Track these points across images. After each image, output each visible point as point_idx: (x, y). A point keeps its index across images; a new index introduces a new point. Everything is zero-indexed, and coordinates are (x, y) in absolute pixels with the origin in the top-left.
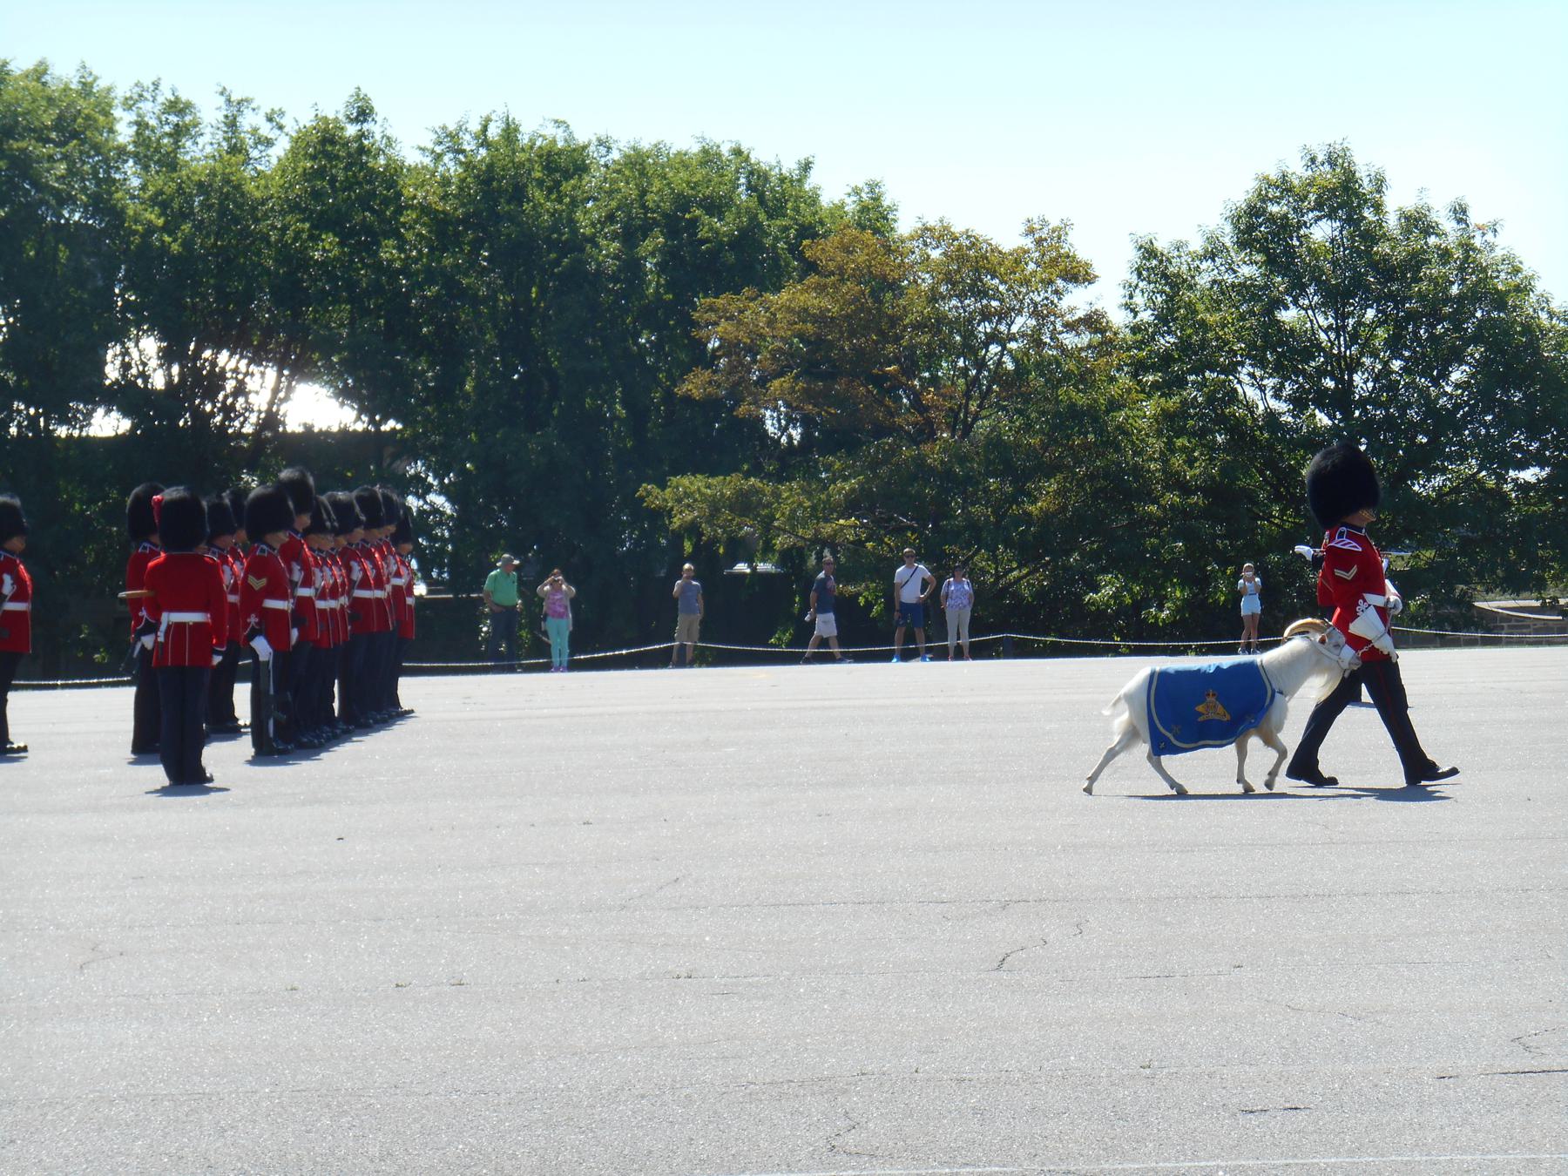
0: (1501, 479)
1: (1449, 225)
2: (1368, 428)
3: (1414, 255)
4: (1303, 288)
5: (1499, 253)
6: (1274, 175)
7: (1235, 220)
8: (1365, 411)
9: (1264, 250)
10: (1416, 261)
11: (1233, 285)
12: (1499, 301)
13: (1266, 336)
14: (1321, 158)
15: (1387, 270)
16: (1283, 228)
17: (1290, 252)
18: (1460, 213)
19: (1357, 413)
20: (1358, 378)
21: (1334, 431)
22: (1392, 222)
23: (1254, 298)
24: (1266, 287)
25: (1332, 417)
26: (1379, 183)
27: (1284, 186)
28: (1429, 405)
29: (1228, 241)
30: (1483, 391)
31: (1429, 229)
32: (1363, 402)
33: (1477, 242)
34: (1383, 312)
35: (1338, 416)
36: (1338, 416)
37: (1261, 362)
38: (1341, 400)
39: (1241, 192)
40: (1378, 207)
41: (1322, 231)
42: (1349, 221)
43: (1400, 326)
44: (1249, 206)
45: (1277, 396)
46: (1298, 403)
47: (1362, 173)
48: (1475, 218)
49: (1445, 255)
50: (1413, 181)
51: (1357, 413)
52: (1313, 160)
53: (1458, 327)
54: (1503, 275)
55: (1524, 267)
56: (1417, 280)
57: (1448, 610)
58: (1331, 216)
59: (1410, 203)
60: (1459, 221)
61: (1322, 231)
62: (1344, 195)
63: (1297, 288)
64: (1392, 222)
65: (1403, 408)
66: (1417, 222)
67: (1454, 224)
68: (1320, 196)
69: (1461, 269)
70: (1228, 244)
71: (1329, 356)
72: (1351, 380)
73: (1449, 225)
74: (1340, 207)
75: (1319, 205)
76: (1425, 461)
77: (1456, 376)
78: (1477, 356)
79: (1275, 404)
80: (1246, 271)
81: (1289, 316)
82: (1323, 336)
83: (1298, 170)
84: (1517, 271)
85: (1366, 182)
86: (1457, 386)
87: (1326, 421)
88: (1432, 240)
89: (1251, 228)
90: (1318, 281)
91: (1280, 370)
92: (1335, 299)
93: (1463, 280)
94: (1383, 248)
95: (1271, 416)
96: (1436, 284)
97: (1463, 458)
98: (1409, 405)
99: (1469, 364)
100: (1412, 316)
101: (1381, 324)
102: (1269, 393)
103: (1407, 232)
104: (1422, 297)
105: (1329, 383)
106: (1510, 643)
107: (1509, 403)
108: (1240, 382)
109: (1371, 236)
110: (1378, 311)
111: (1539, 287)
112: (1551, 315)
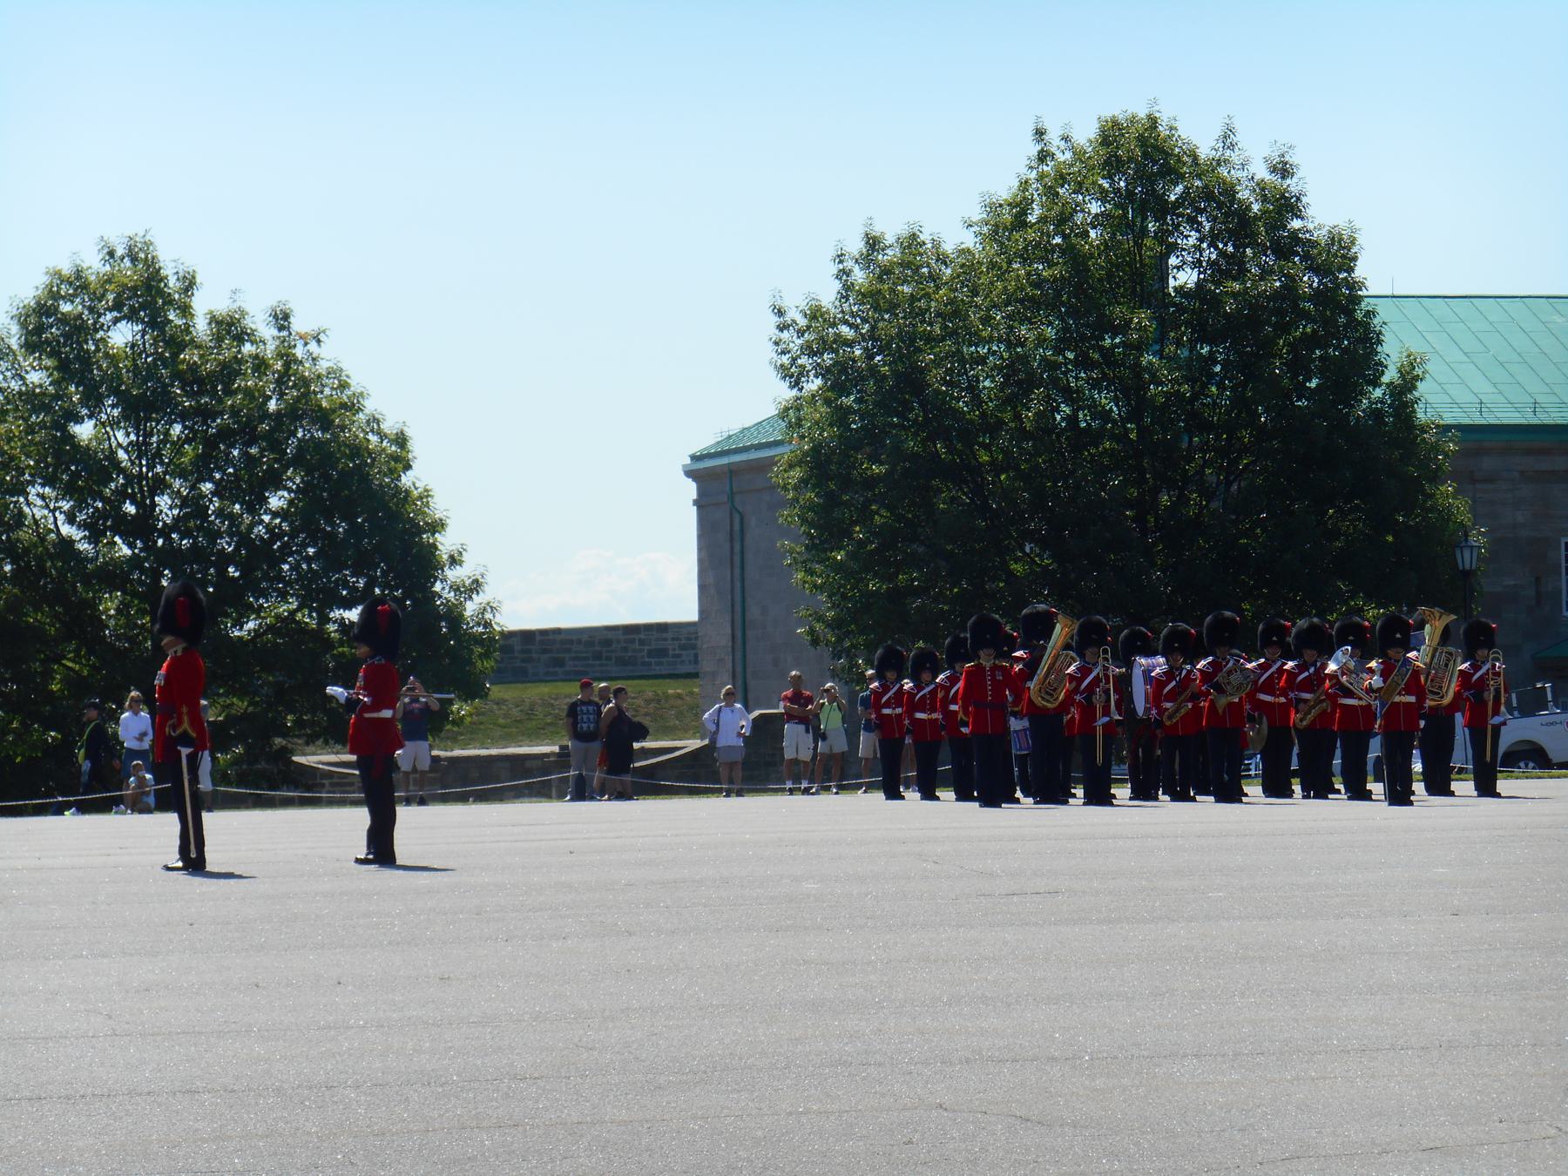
0: (324, 619)
1: (267, 332)
2: (171, 557)
3: (224, 365)
4: (99, 401)
5: (323, 366)
6: (67, 269)
7: (23, 319)
8: (168, 539)
9: (54, 354)
10: (229, 371)
11: (20, 393)
12: (323, 419)
13: (58, 454)
14: (120, 252)
15: (194, 380)
16: (77, 329)
17: (86, 360)
18: (282, 319)
19: (160, 542)
20: (163, 501)
21: (134, 562)
22: (201, 327)
23: (47, 408)
24: (57, 397)
25: (131, 546)
26: (189, 284)
27: (78, 282)
28: (244, 540)
29: (14, 343)
30: (304, 516)
31: (242, 336)
32: (166, 532)
33: (299, 352)
34: (191, 429)
35: (139, 544)
36: (139, 544)
37: (49, 481)
38: (141, 527)
39: (28, 288)
40: (185, 310)
41: (122, 335)
42: (153, 324)
43: (210, 443)
44: (38, 303)
45: (71, 519)
46: (95, 532)
47: (168, 270)
48: (298, 325)
49: (260, 365)
50: (228, 279)
51: (160, 542)
52: (111, 254)
53: (276, 446)
54: (327, 391)
55: (352, 382)
56: (229, 392)
57: (262, 765)
58: (132, 317)
59: (222, 306)
60: (281, 328)
61: (122, 335)
62: (147, 292)
63: (93, 401)
64: (201, 327)
65: (214, 535)
66: (230, 328)
67: (275, 332)
68: (119, 295)
69: (279, 382)
70: (15, 347)
71: (130, 479)
72: (154, 505)
73: (267, 332)
74: (143, 307)
75: (117, 306)
76: (236, 600)
77: (276, 501)
78: (298, 480)
79: (66, 530)
80: (35, 377)
81: (84, 431)
82: (122, 455)
83: (95, 265)
84: (344, 386)
85: (172, 282)
86: (275, 514)
87: (126, 551)
88: (248, 348)
89: (40, 329)
90: (115, 392)
91: (69, 490)
92: (137, 411)
93: (282, 394)
94: (189, 356)
95: (68, 543)
96: (253, 398)
97: (283, 596)
98: (219, 535)
99: (290, 490)
100: (225, 435)
101: (188, 441)
102: (61, 518)
103: (219, 339)
104: (235, 412)
105: (130, 509)
106: (331, 803)
107: (333, 535)
108: (29, 504)
109: (177, 342)
110: (185, 427)
111: (370, 406)
112: (382, 436)
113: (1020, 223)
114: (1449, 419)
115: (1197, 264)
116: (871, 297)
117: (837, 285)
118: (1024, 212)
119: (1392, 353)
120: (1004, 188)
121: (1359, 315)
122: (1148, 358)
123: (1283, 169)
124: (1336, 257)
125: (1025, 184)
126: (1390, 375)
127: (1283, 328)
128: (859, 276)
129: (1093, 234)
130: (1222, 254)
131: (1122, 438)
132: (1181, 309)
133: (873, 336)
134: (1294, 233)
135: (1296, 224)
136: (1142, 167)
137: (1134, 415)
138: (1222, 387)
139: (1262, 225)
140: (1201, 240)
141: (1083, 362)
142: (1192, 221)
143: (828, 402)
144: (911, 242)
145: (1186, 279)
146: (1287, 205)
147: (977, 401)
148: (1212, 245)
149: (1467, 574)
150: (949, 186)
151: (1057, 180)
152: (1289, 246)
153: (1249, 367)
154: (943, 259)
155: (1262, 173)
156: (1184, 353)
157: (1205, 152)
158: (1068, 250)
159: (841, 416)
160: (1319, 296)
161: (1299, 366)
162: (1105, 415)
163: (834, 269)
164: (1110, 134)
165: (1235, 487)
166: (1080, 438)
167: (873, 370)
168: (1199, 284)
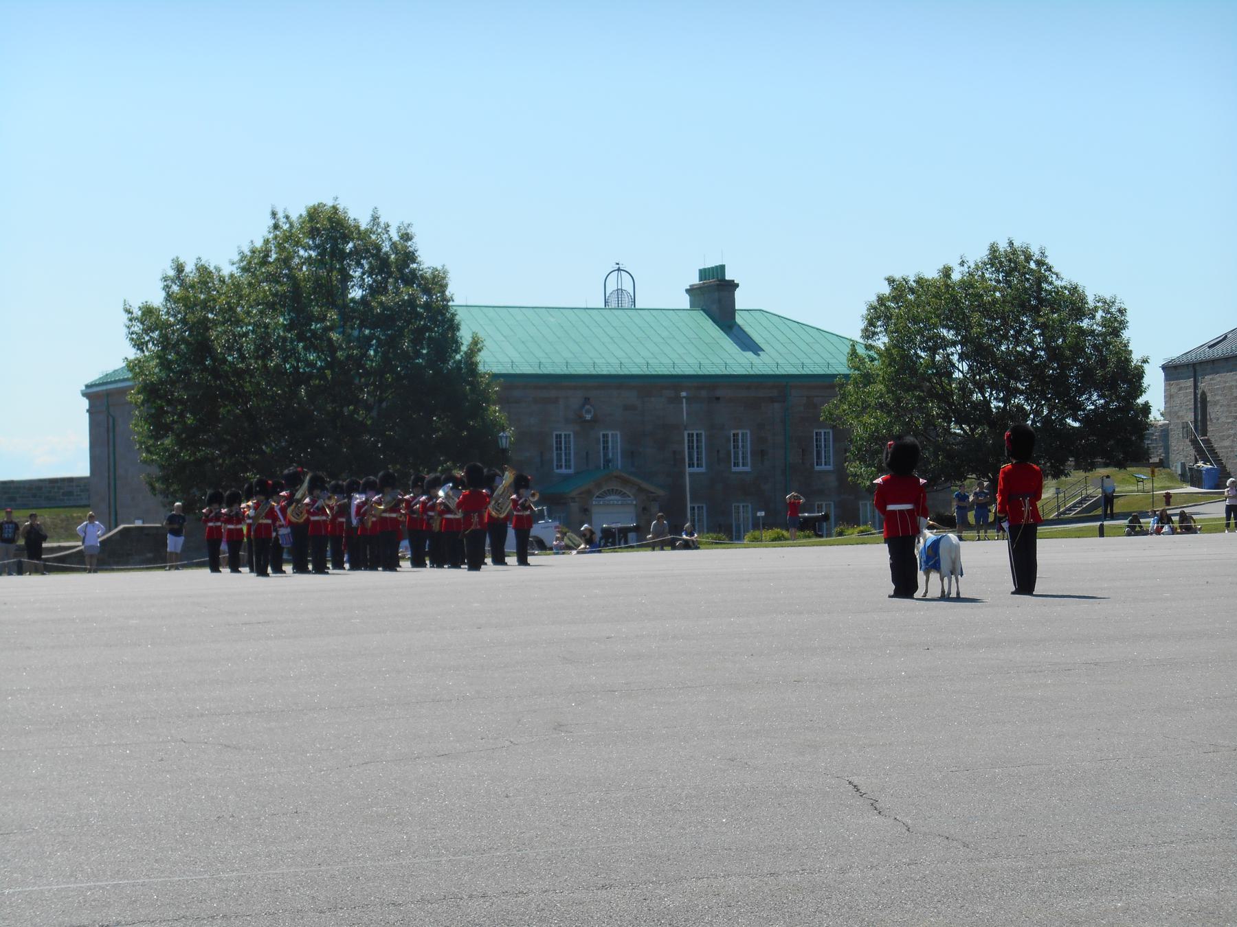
113: (264, 262)
114: (496, 370)
115: (361, 287)
116: (184, 300)
117: (163, 294)
118: (267, 256)
119: (465, 336)
120: (259, 244)
121: (448, 315)
122: (334, 336)
123: (407, 237)
124: (435, 284)
125: (267, 242)
126: (464, 348)
127: (409, 322)
128: (175, 288)
129: (304, 268)
130: (375, 281)
131: (322, 376)
132: (353, 310)
133: (184, 321)
134: (413, 272)
135: (415, 266)
136: (329, 231)
137: (330, 366)
138: (376, 351)
139: (396, 264)
140: (363, 274)
141: (301, 337)
142: (359, 264)
143: (159, 357)
144: (203, 271)
145: (356, 293)
146: (410, 257)
147: (242, 358)
148: (370, 275)
149: (504, 451)
150: (225, 241)
151: (285, 239)
152: (412, 279)
153: (391, 343)
154: (222, 281)
155: (396, 238)
156: (356, 333)
157: (363, 227)
158: (291, 277)
159: (165, 364)
160: (427, 306)
161: (417, 341)
162: (311, 364)
163: (161, 285)
164: (314, 214)
165: (384, 405)
166: (299, 378)
167: (184, 340)
168: (363, 297)
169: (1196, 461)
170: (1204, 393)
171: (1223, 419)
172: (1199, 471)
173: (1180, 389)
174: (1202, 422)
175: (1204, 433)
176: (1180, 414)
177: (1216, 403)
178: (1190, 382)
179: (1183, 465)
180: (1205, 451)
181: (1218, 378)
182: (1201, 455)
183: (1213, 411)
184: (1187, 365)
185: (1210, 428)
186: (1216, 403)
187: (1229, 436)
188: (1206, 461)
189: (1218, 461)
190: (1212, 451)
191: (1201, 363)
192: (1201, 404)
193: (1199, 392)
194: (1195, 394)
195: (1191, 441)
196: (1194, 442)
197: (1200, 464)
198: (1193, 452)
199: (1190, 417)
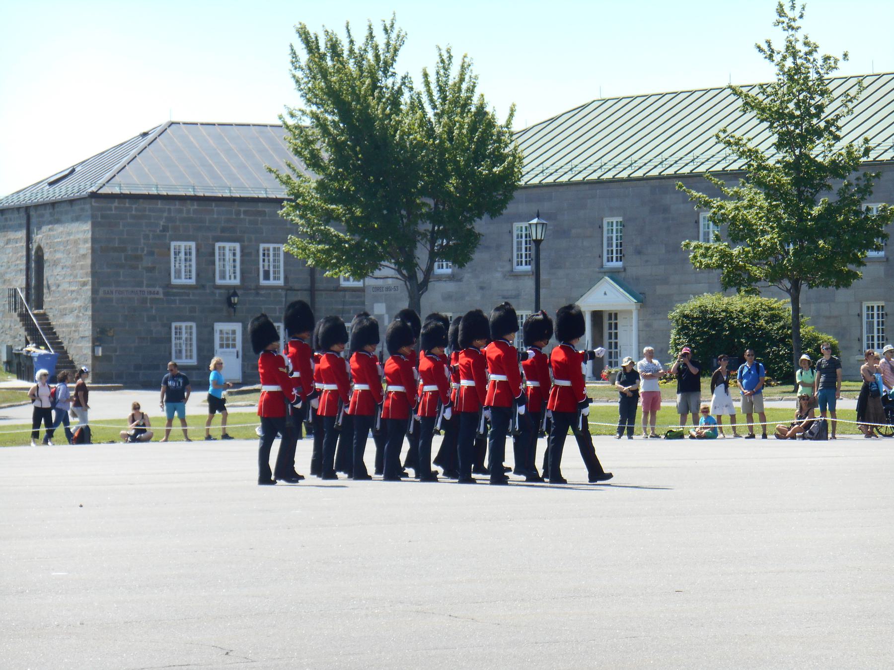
169: (27, 343)
170: (39, 249)
171: (65, 286)
172: (29, 358)
173: (8, 242)
174: (36, 289)
175: (39, 304)
176: (8, 277)
177: (55, 263)
178: (22, 234)
179: (10, 349)
180: (40, 330)
181: (59, 228)
182: (34, 336)
183: (50, 275)
184: (18, 209)
185: (47, 298)
186: (55, 263)
187: (72, 311)
188: (39, 343)
189: (57, 345)
190: (49, 330)
191: (37, 206)
192: (36, 264)
193: (34, 247)
194: (28, 250)
195: (20, 315)
196: (25, 318)
197: (31, 348)
198: (23, 332)
199: (19, 282)
